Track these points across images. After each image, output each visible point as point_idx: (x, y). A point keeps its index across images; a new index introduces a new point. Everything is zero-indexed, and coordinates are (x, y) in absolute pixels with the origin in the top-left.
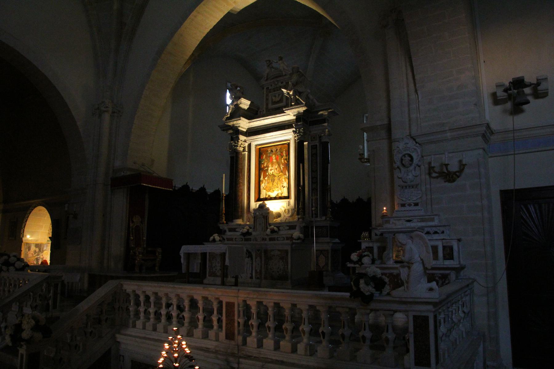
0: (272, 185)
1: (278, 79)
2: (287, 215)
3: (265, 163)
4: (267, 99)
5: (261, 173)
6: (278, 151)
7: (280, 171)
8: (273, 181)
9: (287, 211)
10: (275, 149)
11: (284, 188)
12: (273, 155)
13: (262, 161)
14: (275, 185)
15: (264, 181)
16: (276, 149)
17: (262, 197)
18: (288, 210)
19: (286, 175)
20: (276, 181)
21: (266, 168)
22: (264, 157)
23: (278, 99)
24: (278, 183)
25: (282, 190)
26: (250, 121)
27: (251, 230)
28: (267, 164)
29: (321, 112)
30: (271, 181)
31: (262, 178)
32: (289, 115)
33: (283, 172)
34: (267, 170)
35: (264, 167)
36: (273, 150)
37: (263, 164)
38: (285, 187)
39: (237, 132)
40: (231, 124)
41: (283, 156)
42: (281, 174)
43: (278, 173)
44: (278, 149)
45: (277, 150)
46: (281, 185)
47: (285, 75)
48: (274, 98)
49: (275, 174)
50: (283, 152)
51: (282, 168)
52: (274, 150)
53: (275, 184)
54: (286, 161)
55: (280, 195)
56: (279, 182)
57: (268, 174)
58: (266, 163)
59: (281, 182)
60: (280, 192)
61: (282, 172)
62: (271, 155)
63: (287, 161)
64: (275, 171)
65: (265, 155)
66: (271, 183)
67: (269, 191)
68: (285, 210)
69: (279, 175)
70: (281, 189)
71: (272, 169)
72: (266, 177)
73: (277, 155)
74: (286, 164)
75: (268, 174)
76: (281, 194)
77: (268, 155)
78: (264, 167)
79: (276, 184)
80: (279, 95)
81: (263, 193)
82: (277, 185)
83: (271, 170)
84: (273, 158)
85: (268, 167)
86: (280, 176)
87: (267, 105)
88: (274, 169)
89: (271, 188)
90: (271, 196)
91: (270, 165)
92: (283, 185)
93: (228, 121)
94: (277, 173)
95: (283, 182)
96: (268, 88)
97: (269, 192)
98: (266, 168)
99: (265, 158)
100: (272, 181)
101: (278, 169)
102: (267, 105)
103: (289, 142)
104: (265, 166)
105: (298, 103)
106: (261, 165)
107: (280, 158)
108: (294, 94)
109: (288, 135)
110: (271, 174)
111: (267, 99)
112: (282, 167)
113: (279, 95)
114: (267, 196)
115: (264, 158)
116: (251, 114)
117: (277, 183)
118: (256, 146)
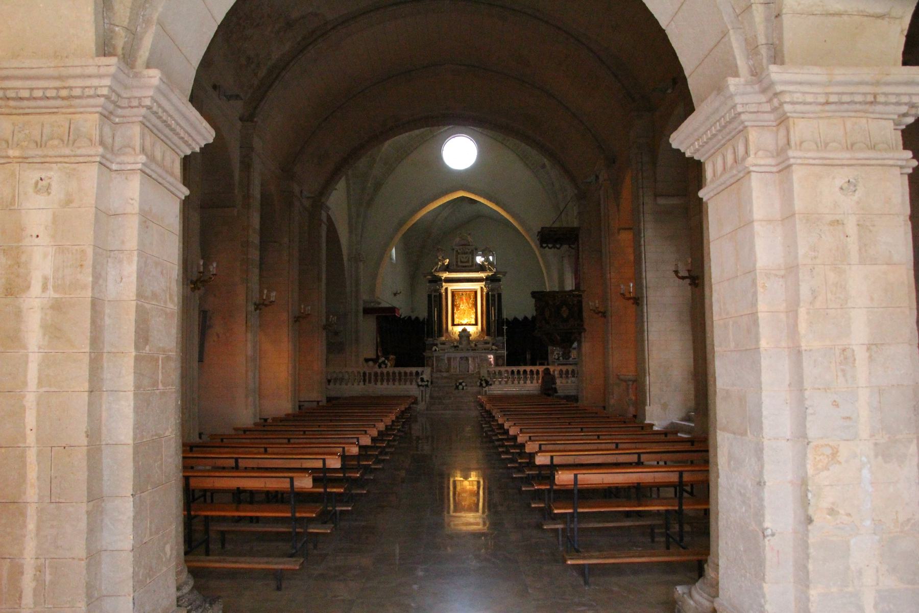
1: (467, 247)
2: (476, 336)
4: (457, 258)
17: (455, 323)
20: (466, 313)
23: (466, 260)
27: (458, 345)
31: (455, 311)
32: (482, 275)
39: (440, 279)
47: (472, 245)
53: (465, 315)
55: (469, 323)
80: (466, 257)
85: (460, 304)
87: (457, 262)
96: (457, 251)
102: (457, 262)
105: (491, 270)
108: (488, 264)
109: (477, 286)
111: (457, 258)
112: (470, 305)
113: (466, 257)
116: (447, 269)
118: (452, 290)
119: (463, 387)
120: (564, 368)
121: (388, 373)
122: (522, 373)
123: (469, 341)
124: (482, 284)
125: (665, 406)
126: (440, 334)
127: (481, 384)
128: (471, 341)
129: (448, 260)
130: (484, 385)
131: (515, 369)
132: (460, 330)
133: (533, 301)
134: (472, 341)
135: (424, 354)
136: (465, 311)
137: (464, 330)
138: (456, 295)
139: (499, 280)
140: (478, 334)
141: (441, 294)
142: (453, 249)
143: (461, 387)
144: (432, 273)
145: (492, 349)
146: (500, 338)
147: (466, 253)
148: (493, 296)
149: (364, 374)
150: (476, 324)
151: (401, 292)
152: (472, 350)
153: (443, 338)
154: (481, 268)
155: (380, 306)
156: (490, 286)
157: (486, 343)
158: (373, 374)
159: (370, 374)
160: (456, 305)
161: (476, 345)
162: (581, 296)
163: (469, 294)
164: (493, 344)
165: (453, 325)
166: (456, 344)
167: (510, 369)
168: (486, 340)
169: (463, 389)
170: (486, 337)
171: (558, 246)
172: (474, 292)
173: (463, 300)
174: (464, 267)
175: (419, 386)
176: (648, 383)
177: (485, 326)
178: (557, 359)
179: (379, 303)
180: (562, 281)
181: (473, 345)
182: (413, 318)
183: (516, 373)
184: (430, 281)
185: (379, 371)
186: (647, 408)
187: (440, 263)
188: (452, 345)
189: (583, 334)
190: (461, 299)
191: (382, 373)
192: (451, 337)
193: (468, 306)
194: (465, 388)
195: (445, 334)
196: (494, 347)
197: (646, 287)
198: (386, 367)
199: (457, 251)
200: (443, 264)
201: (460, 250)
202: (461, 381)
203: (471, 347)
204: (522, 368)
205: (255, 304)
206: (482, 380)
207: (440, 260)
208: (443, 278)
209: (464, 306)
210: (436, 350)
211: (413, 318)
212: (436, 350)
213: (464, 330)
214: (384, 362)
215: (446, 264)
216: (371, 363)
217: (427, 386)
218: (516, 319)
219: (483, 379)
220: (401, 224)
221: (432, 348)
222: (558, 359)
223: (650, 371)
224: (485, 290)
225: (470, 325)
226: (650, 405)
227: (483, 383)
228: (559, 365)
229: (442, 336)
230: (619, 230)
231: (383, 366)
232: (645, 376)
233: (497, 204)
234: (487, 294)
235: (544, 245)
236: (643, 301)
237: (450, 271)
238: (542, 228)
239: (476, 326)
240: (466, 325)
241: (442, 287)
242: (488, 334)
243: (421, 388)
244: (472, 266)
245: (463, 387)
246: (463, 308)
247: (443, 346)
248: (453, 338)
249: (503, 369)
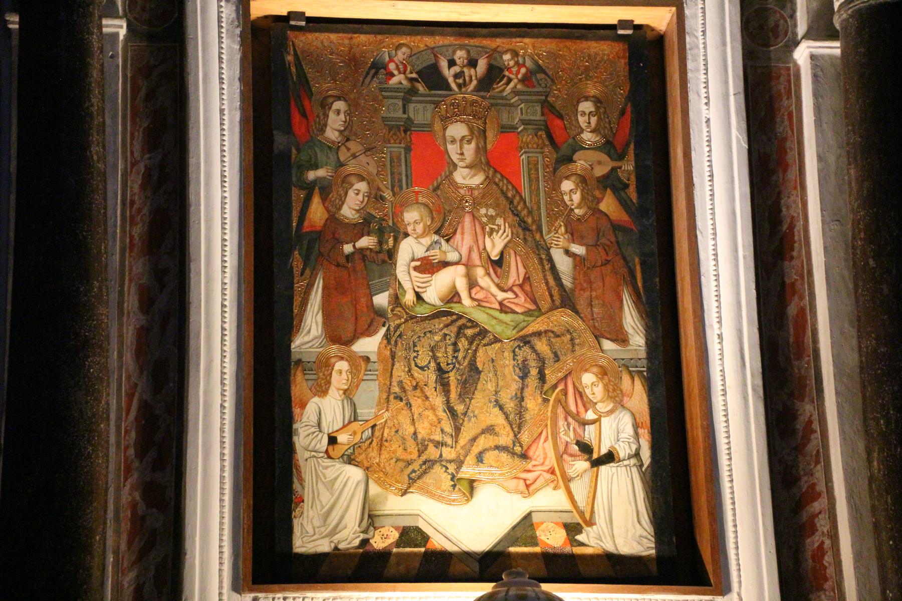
0: (448, 428)
3: (345, 182)
5: (299, 285)
6: (506, 89)
7: (541, 290)
8: (453, 377)
10: (473, 63)
11: (604, 469)
12: (446, 120)
13: (316, 167)
14: (490, 430)
16: (482, 65)
19: (621, 339)
21: (366, 242)
24: (521, 411)
25: (580, 489)
28: (376, 197)
30: (431, 376)
33: (582, 305)
36: (448, 73)
38: (610, 458)
41: (577, 147)
42: (563, 318)
43: (521, 303)
44: (515, 77)
45: (494, 74)
46: (567, 436)
49: (480, 316)
51: (563, 264)
54: (608, 204)
56: (532, 403)
57: (396, 300)
58: (362, 186)
59: (562, 402)
61: (567, 301)
62: (420, 113)
63: (624, 203)
64: (484, 281)
65: (340, 105)
66: (438, 401)
69: (535, 327)
70: (567, 480)
71: (436, 255)
72: (369, 332)
73: (506, 129)
74: (616, 227)
75: (396, 300)
76: (572, 529)
78: (333, 219)
79: (496, 418)
81: (326, 498)
82: (517, 423)
83: (428, 267)
84: (453, 150)
86: (542, 346)
88: (469, 266)
89: (432, 452)
90: (438, 542)
91: (412, 216)
92: (589, 434)
94: (503, 308)
95: (587, 404)
97: (404, 493)
98: (366, 242)
99: (348, 133)
100: (444, 384)
101: (515, 271)
104: (349, 211)
106: (298, 195)
107: (533, 166)
110: (422, 311)
115: (332, 134)
117: (510, 406)
138: (321, 85)
193: (515, 271)
246: (434, 292)
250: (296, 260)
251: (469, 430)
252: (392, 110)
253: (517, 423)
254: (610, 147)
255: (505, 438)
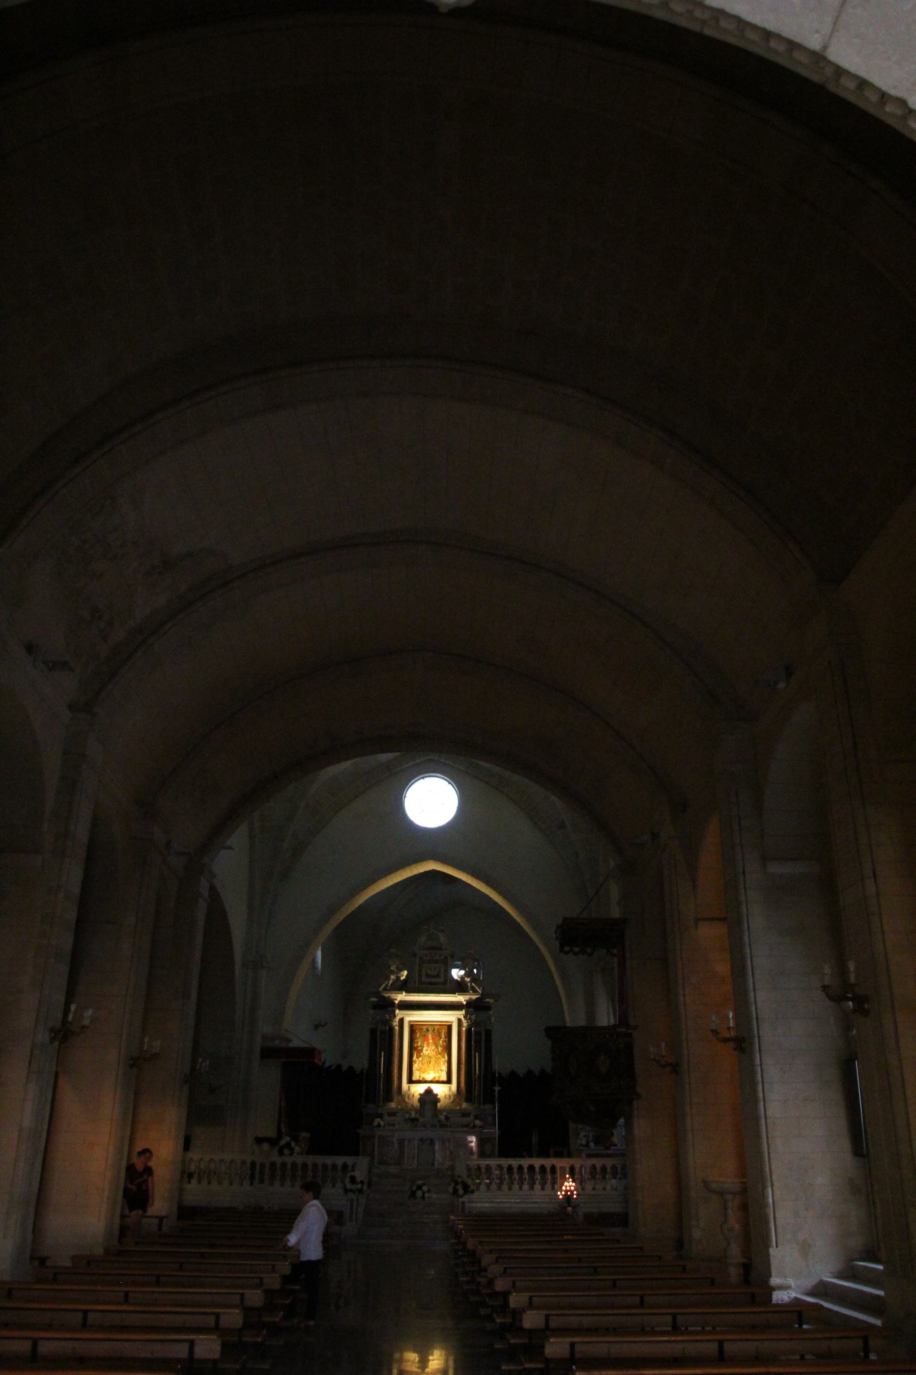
2: (447, 1101)
4: (420, 971)
6: (435, 1031)
9: (448, 1096)
15: (417, 1062)
17: (415, 1078)
18: (450, 1096)
19: (445, 1058)
21: (420, 1048)
22: (418, 1035)
26: (407, 994)
27: (417, 1116)
28: (422, 1043)
29: (488, 1000)
31: (415, 1058)
32: (461, 998)
34: (422, 1050)
35: (418, 1047)
37: (417, 1042)
40: (386, 995)
42: (439, 1056)
43: (435, 1054)
45: (434, 1029)
47: (445, 949)
48: (428, 971)
50: (441, 1033)
51: (440, 1050)
52: (430, 1028)
53: (431, 1065)
54: (445, 1044)
55: (437, 1079)
60: (437, 1075)
61: (440, 1054)
67: (424, 1072)
68: (445, 1096)
69: (437, 1057)
72: (420, 1057)
76: (439, 1078)
77: (423, 1033)
82: (434, 1067)
83: (426, 1050)
85: (423, 1047)
87: (420, 976)
91: (425, 1045)
93: (386, 992)
96: (421, 958)
98: (420, 1048)
99: (419, 1036)
101: (435, 1051)
102: (420, 976)
103: (450, 1024)
105: (475, 991)
108: (471, 981)
111: (420, 971)
112: (440, 1049)
114: (421, 1079)
116: (405, 987)
118: (410, 1022)
119: (424, 1193)
120: (598, 1163)
121: (294, 1165)
122: (526, 1170)
123: (436, 1111)
124: (461, 1014)
125: (805, 1248)
126: (388, 1098)
127: (455, 1191)
128: (439, 1110)
129: (405, 973)
130: (461, 1192)
131: (515, 1162)
132: (422, 1091)
133: (549, 1043)
134: (441, 1111)
135: (359, 1131)
136: (430, 1057)
137: (429, 1092)
139: (488, 1008)
140: (452, 1100)
141: (392, 1029)
142: (415, 955)
143: (419, 1193)
144: (379, 992)
145: (474, 1126)
146: (488, 1106)
147: (436, 962)
148: (478, 1033)
149: (253, 1164)
150: (449, 1081)
151: (326, 1024)
152: (442, 1126)
153: (393, 1105)
154: (459, 987)
155: (291, 1045)
156: (473, 1017)
157: (465, 1114)
158: (268, 1166)
159: (262, 1165)
160: (416, 1048)
161: (447, 1118)
162: (631, 1035)
163: (438, 1030)
164: (476, 1117)
165: (411, 1081)
166: (413, 1115)
167: (505, 1162)
168: (465, 1109)
169: (423, 1197)
170: (464, 1105)
171: (589, 950)
172: (446, 1027)
173: (427, 1039)
174: (431, 984)
175: (346, 1191)
176: (771, 1201)
177: (463, 1085)
178: (584, 1146)
179: (289, 1041)
180: (591, 1014)
181: (442, 1117)
182: (345, 1068)
183: (515, 1170)
184: (376, 1007)
185: (278, 1160)
186: (772, 1251)
187: (392, 977)
188: (407, 1116)
189: (635, 1103)
190: (426, 1038)
191: (284, 1165)
192: (407, 1103)
194: (426, 1195)
195: (396, 1098)
196: (478, 1122)
197: (757, 1018)
198: (291, 1154)
199: (421, 958)
200: (398, 978)
201: (426, 956)
202: (420, 1182)
203: (439, 1121)
204: (526, 1162)
205: (52, 1030)
206: (457, 1183)
207: (392, 972)
208: (397, 1002)
209: (428, 1050)
210: (379, 1125)
211: (345, 1068)
212: (379, 1125)
213: (429, 1092)
214: (288, 1145)
215: (402, 978)
216: (266, 1146)
217: (360, 1191)
218: (513, 1073)
219: (460, 1180)
220: (333, 910)
221: (373, 1121)
222: (587, 1145)
223: (774, 1177)
224: (465, 1024)
225: (438, 1082)
226: (777, 1247)
227: (460, 1187)
228: (589, 1156)
229: (391, 1100)
230: (697, 921)
231: (286, 1151)
232: (764, 1187)
233: (487, 882)
234: (469, 1031)
235: (567, 949)
236: (752, 1044)
237: (409, 991)
238: (565, 919)
239: (449, 1085)
240: (431, 1082)
241: (395, 1016)
242: (469, 1099)
243: (351, 1195)
244: (445, 983)
245: (424, 1193)
246: (427, 1053)
247: (391, 1118)
248: (409, 1106)
249: (493, 1162)
250: (414, 1050)
251: (430, 1067)
252: (423, 1033)
253: (434, 1067)
254: (445, 1038)
255: (433, 1068)
